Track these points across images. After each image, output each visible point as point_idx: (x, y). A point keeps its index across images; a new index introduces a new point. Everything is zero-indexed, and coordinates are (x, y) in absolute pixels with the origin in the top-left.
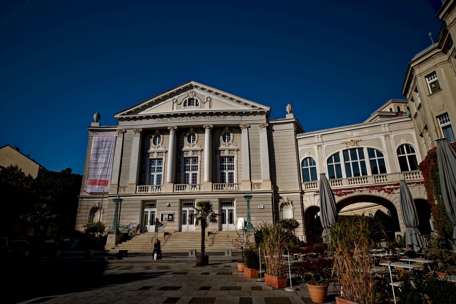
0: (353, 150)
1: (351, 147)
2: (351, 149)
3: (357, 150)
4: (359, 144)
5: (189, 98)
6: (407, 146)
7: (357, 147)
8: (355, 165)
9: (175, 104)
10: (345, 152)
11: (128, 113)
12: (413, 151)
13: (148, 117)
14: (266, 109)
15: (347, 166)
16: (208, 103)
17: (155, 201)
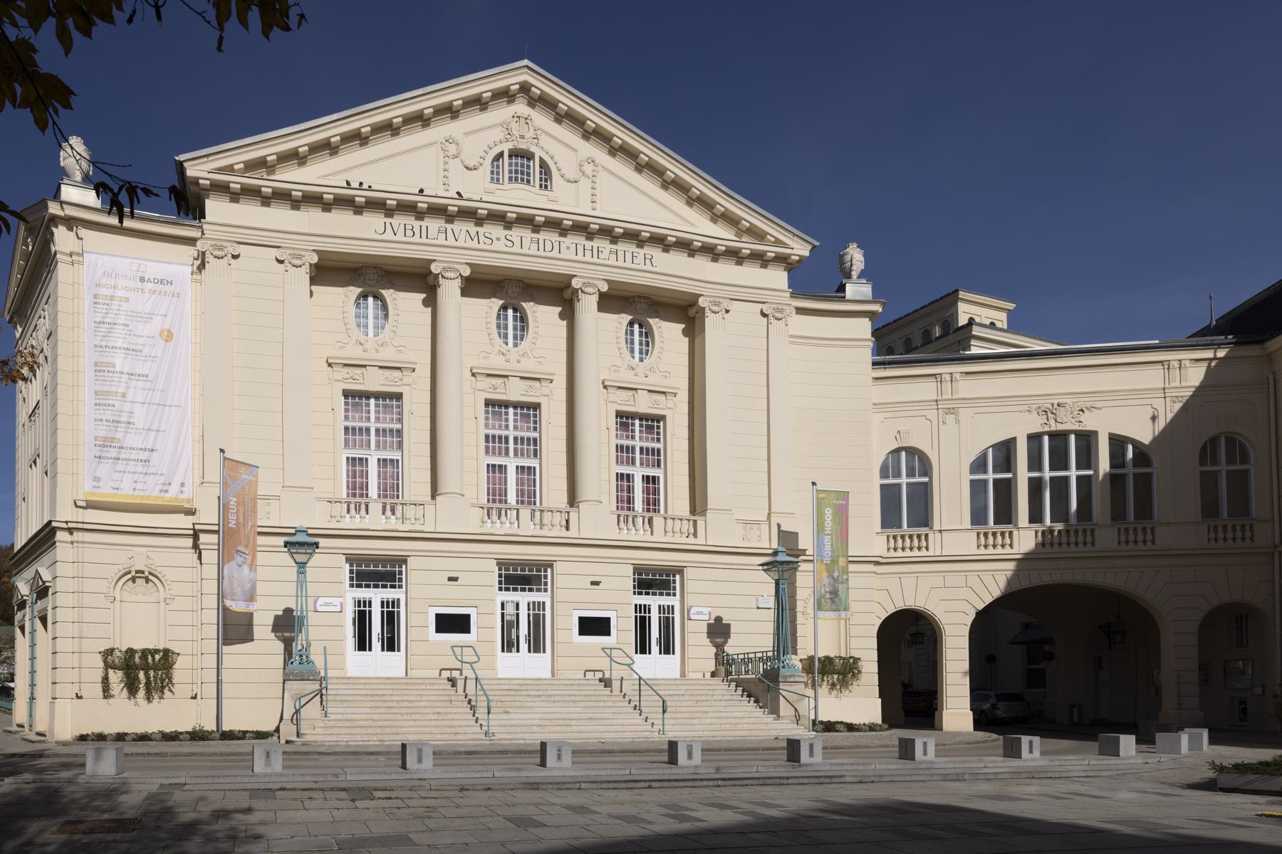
0: (1059, 438)
1: (1054, 427)
2: (1054, 436)
3: (1073, 437)
4: (1083, 417)
5: (510, 145)
6: (1231, 441)
7: (1076, 427)
8: (1060, 486)
9: (455, 165)
10: (1034, 439)
11: (252, 166)
12: (1245, 459)
13: (313, 199)
14: (799, 249)
15: (1035, 487)
16: (585, 184)
17: (402, 561)
